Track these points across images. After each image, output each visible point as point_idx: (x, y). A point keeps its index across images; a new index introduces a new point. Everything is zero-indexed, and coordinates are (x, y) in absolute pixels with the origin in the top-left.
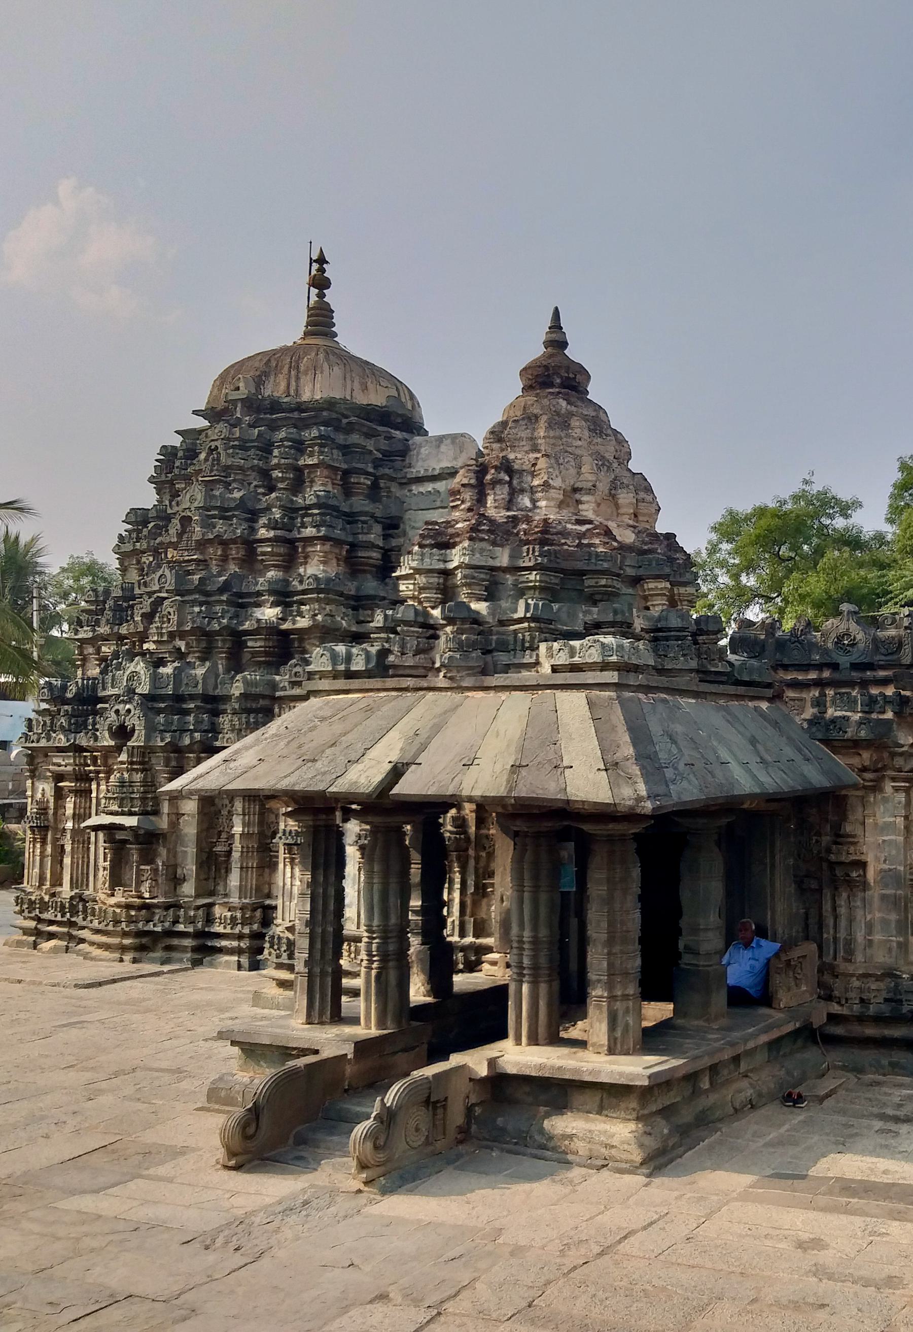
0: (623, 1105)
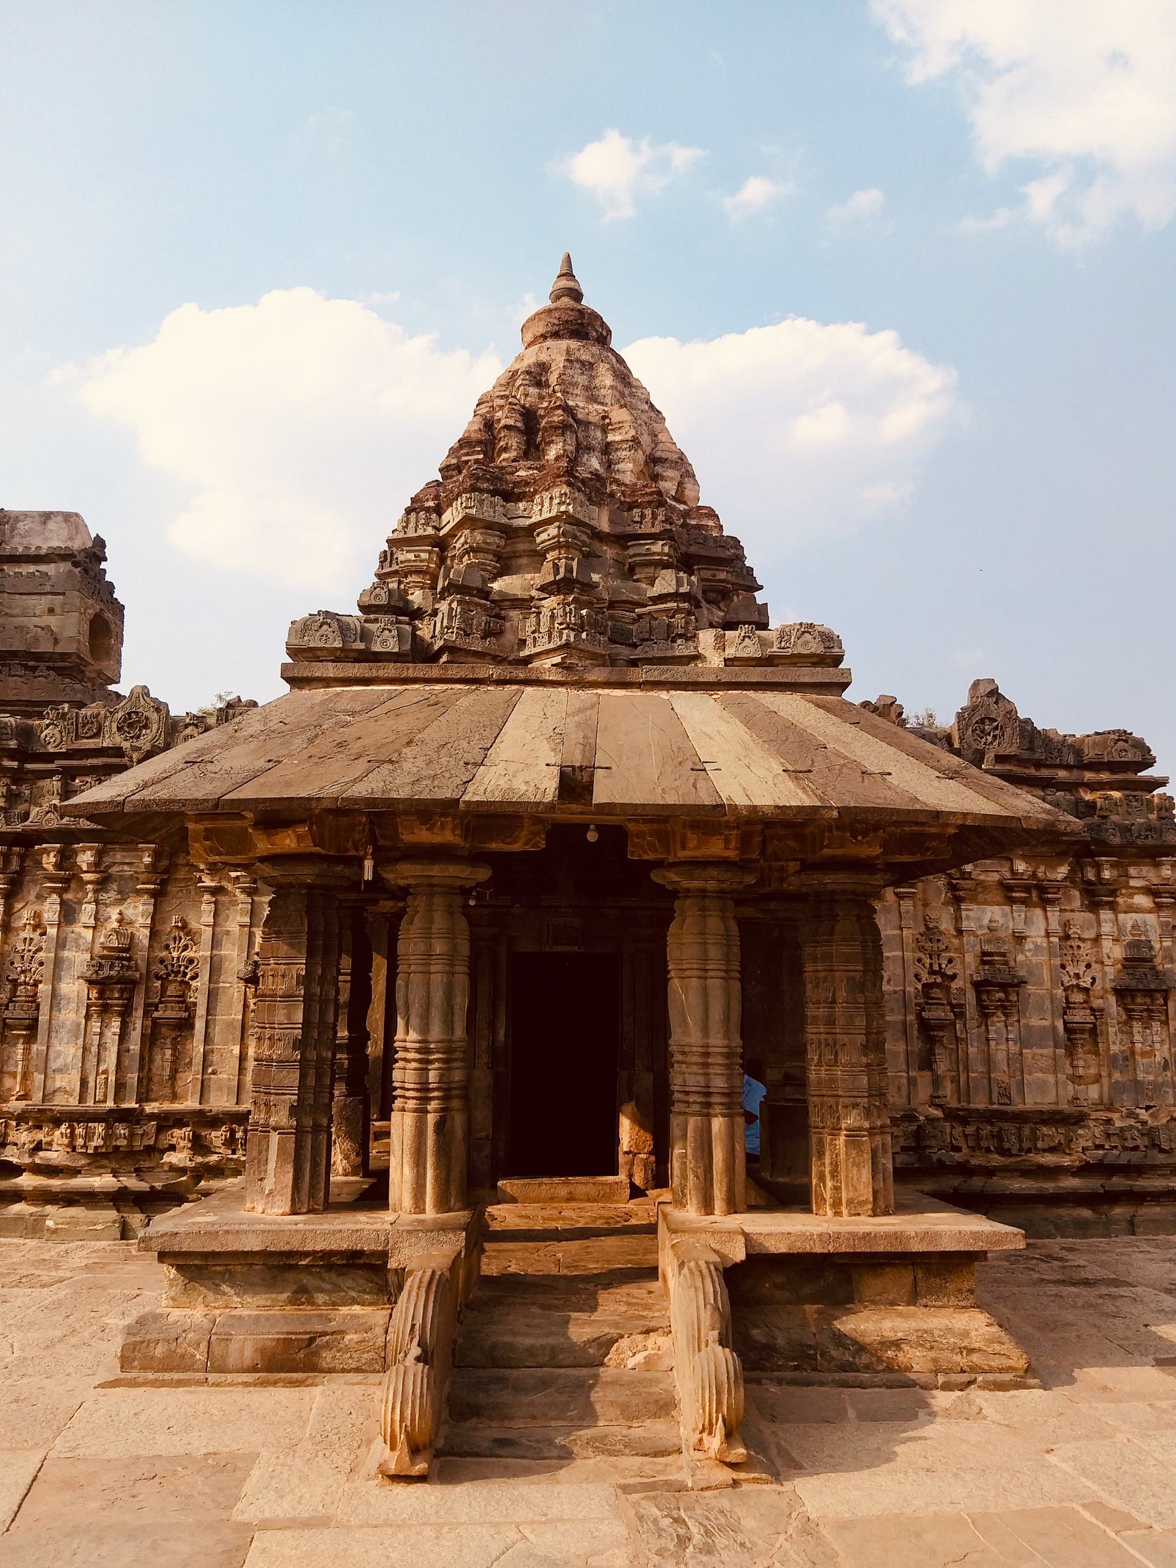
0: (951, 1287)
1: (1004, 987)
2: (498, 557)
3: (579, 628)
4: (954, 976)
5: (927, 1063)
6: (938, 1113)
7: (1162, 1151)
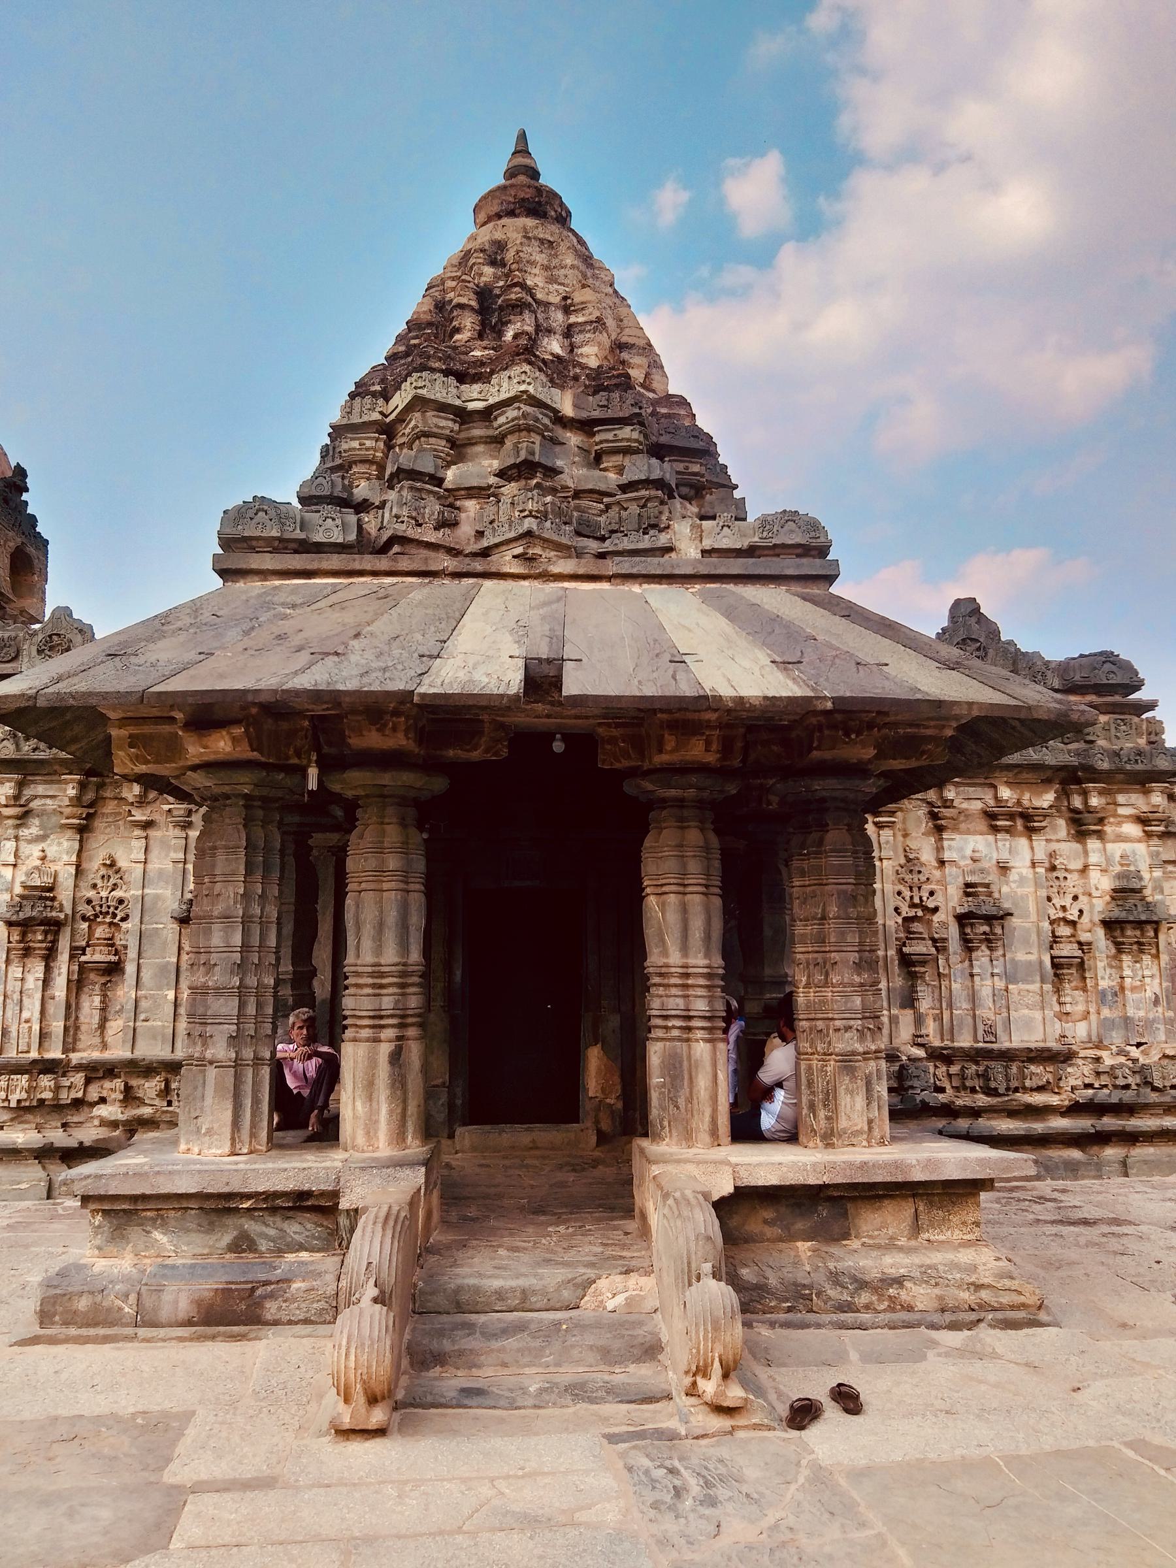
0: (955, 1219)
1: (989, 919)
2: (453, 443)
3: (542, 516)
4: (936, 910)
5: (909, 1001)
6: (921, 1053)
7: (1155, 1089)
